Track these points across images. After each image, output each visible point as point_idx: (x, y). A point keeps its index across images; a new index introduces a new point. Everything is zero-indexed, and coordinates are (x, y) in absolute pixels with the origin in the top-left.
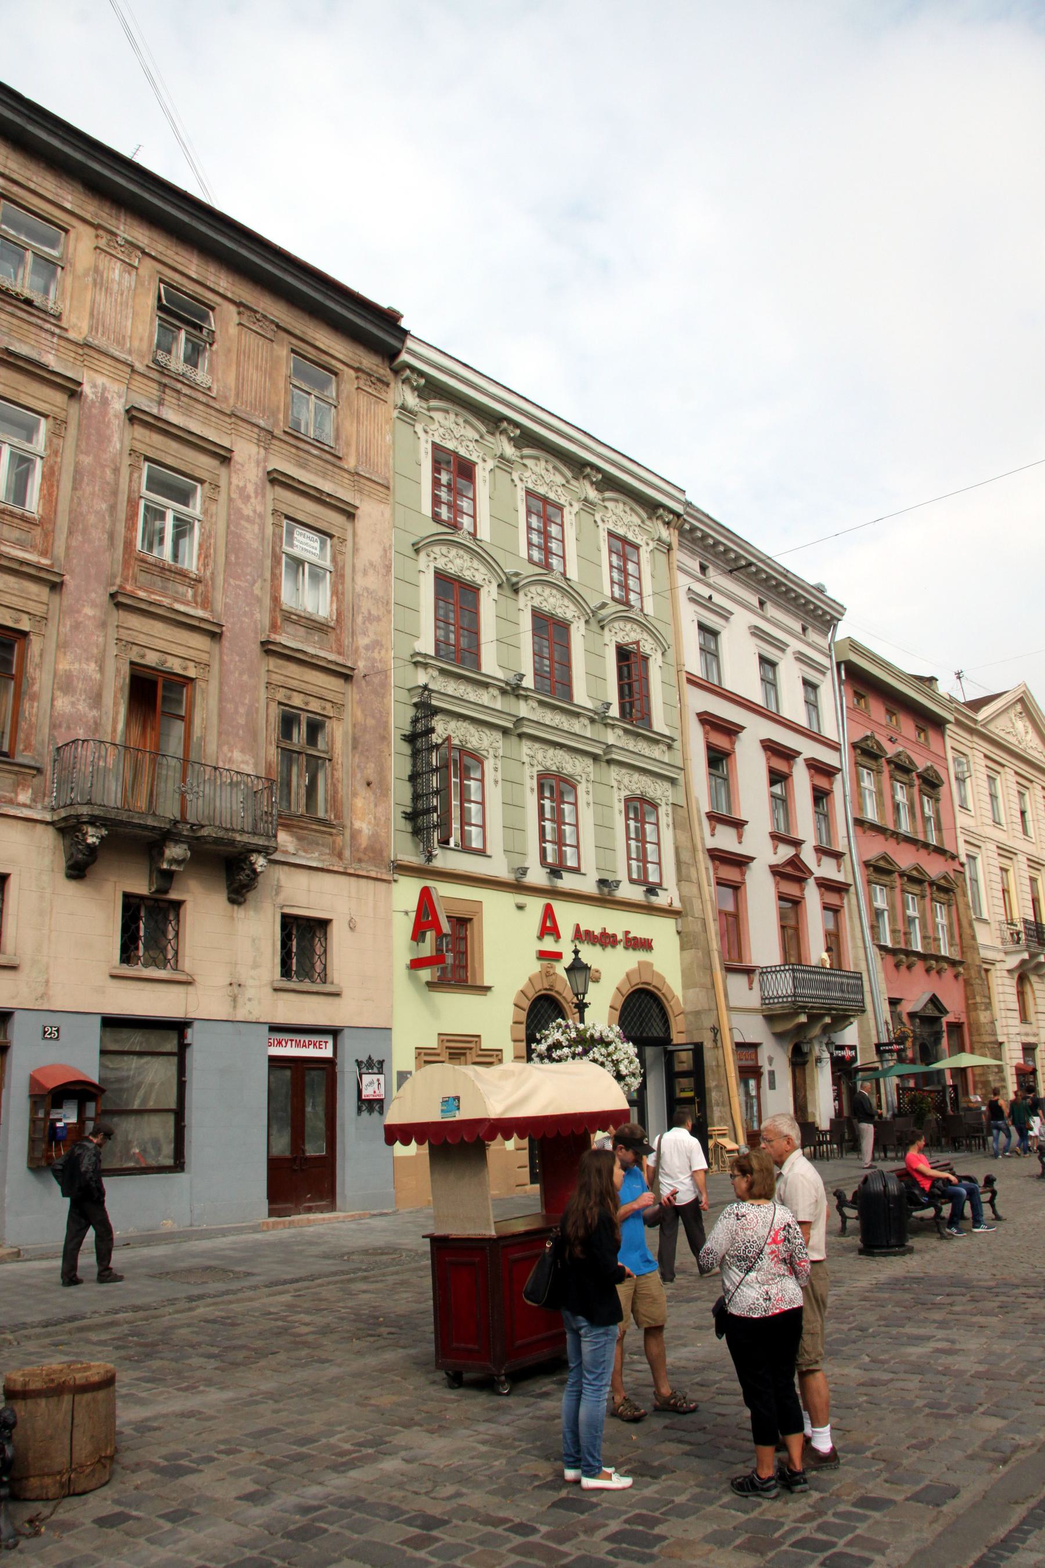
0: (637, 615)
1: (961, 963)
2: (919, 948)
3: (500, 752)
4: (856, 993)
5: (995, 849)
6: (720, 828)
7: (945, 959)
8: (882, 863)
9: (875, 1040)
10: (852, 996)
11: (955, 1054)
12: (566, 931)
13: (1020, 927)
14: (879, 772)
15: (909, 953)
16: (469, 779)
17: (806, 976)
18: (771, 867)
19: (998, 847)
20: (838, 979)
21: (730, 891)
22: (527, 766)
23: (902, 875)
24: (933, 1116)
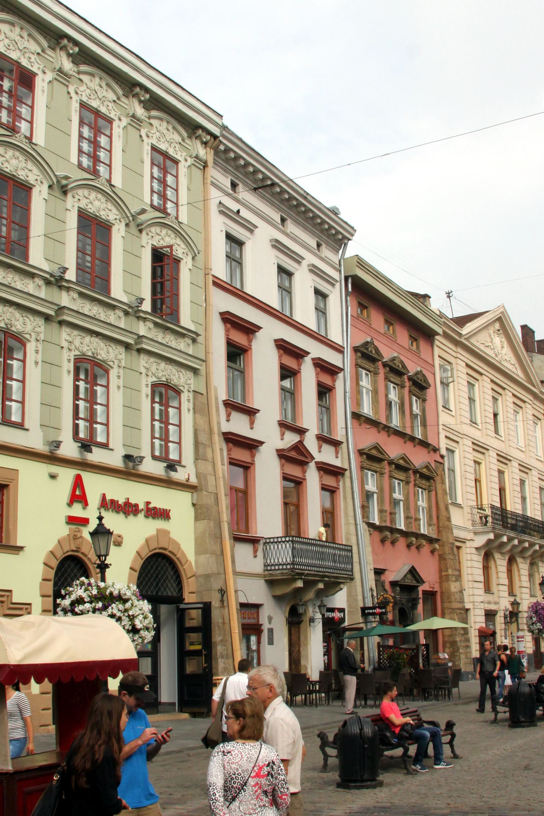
0: (172, 222)
1: (437, 540)
2: (401, 525)
3: (42, 337)
4: (347, 563)
5: (470, 444)
6: (235, 415)
7: (423, 536)
8: (374, 452)
9: (361, 605)
10: (343, 566)
11: (428, 618)
12: (94, 500)
13: (488, 512)
14: (376, 374)
15: (393, 530)
16: (13, 359)
17: (304, 547)
18: (278, 451)
19: (473, 443)
20: (332, 551)
21: (241, 470)
22: (65, 350)
23: (391, 463)
24: (407, 671)
